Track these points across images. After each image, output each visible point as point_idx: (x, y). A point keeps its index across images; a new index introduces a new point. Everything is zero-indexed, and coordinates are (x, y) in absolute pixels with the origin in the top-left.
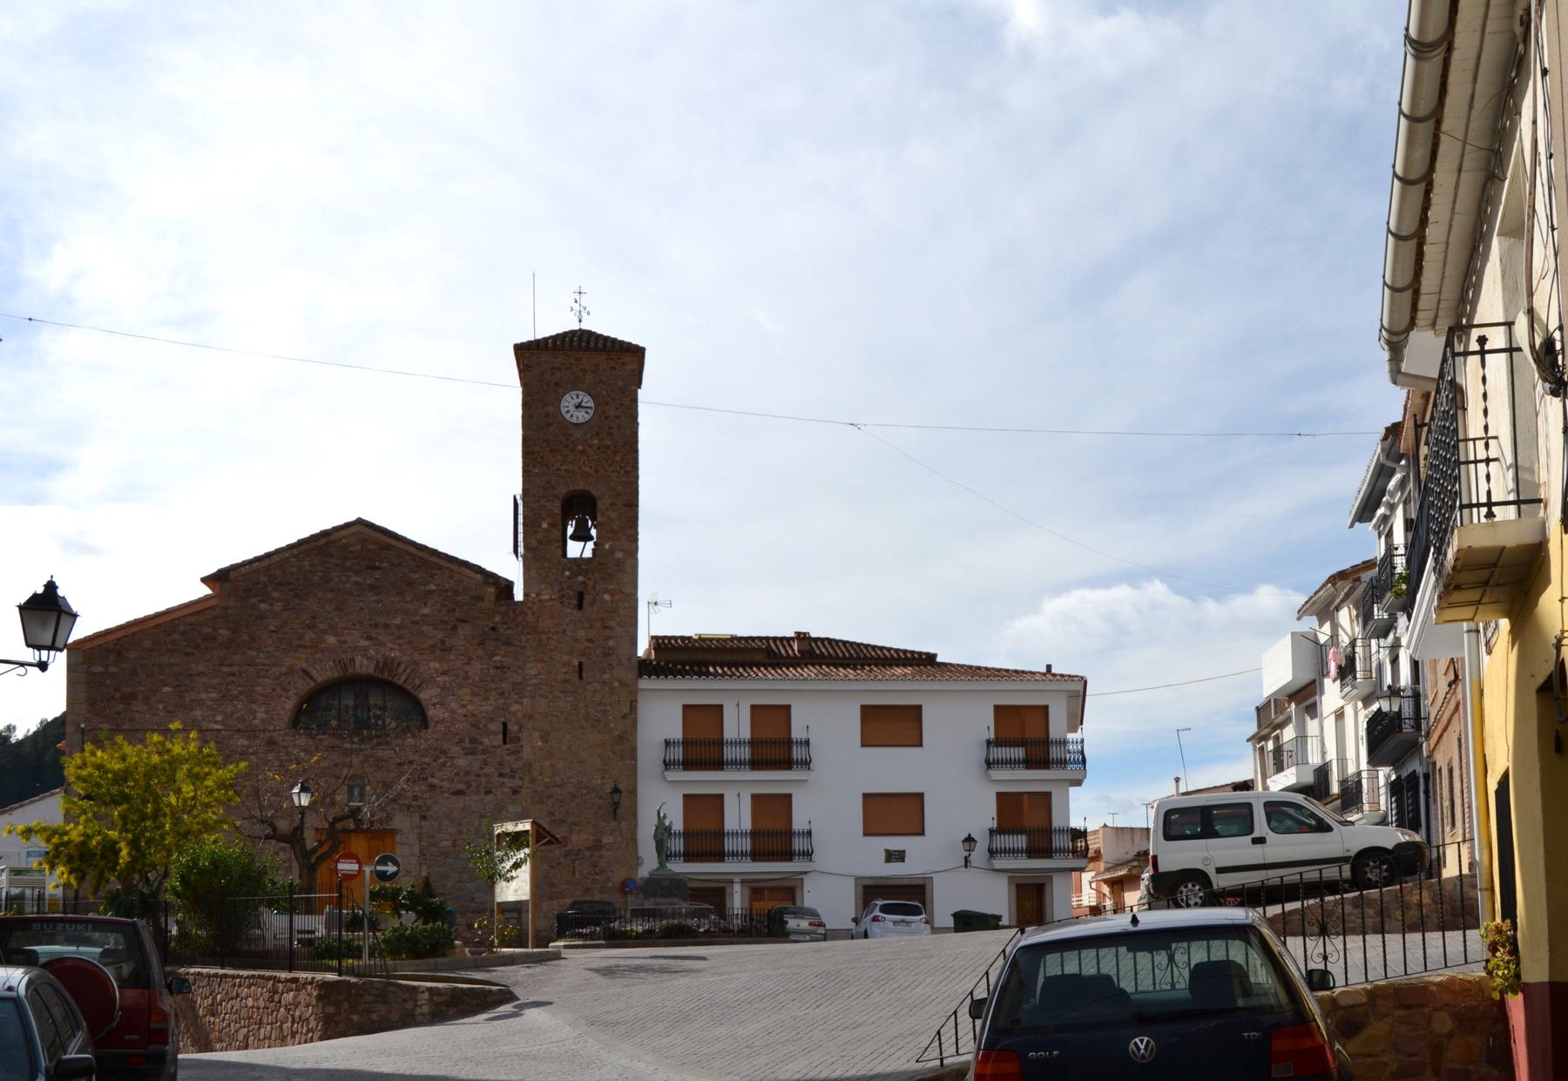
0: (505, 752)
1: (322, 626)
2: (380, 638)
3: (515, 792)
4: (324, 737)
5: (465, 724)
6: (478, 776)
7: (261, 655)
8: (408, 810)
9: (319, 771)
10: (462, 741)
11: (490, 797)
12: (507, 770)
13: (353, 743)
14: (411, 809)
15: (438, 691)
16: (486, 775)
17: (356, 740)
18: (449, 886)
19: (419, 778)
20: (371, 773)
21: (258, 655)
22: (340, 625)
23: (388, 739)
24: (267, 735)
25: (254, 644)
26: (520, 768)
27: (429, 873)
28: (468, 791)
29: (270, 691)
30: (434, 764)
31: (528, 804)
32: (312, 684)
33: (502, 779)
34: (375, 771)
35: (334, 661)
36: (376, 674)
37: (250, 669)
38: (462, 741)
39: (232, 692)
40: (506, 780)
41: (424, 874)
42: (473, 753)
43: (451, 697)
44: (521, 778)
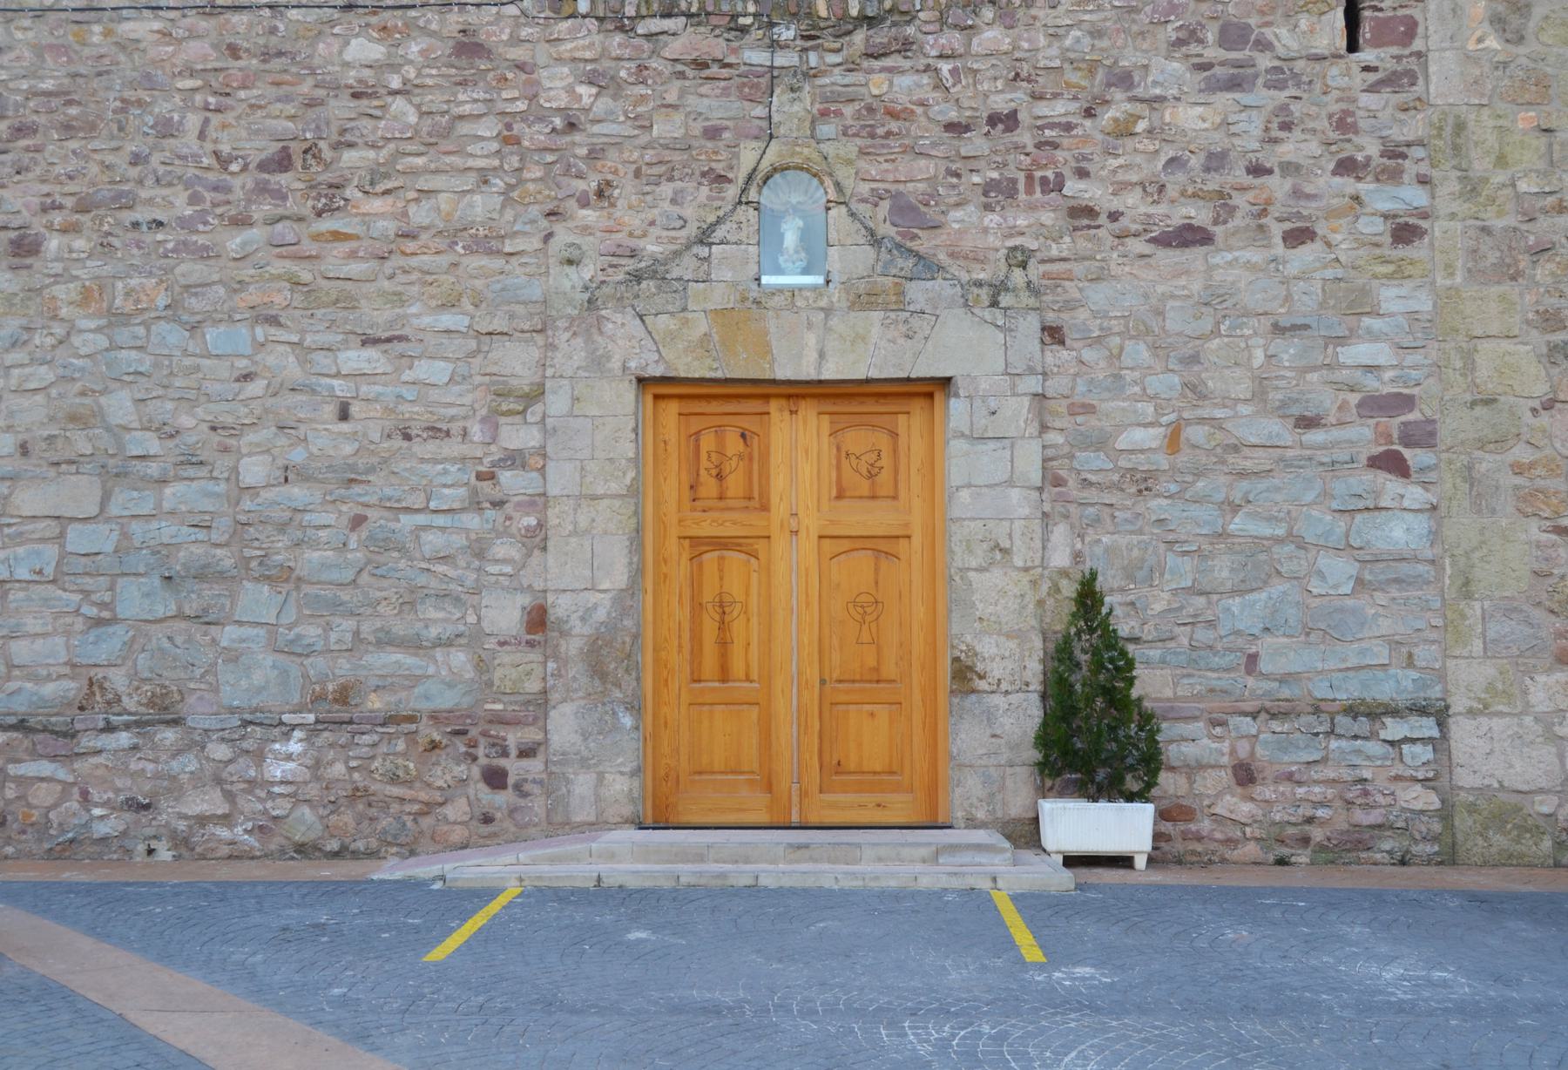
0: (1359, 80)
3: (1405, 233)
4: (668, 24)
6: (1257, 170)
9: (649, 156)
10: (1191, 36)
11: (1307, 254)
12: (1369, 148)
14: (1005, 300)
16: (1289, 168)
17: (786, 33)
18: (1158, 607)
19: (1030, 178)
20: (849, 162)
23: (910, 30)
26: (1420, 143)
28: (1218, 231)
30: (1088, 123)
31: (1458, 279)
33: (1348, 184)
34: (863, 153)
38: (1191, 36)
40: (1365, 187)
41: (1060, 558)
42: (1234, 84)
44: (1423, 181)
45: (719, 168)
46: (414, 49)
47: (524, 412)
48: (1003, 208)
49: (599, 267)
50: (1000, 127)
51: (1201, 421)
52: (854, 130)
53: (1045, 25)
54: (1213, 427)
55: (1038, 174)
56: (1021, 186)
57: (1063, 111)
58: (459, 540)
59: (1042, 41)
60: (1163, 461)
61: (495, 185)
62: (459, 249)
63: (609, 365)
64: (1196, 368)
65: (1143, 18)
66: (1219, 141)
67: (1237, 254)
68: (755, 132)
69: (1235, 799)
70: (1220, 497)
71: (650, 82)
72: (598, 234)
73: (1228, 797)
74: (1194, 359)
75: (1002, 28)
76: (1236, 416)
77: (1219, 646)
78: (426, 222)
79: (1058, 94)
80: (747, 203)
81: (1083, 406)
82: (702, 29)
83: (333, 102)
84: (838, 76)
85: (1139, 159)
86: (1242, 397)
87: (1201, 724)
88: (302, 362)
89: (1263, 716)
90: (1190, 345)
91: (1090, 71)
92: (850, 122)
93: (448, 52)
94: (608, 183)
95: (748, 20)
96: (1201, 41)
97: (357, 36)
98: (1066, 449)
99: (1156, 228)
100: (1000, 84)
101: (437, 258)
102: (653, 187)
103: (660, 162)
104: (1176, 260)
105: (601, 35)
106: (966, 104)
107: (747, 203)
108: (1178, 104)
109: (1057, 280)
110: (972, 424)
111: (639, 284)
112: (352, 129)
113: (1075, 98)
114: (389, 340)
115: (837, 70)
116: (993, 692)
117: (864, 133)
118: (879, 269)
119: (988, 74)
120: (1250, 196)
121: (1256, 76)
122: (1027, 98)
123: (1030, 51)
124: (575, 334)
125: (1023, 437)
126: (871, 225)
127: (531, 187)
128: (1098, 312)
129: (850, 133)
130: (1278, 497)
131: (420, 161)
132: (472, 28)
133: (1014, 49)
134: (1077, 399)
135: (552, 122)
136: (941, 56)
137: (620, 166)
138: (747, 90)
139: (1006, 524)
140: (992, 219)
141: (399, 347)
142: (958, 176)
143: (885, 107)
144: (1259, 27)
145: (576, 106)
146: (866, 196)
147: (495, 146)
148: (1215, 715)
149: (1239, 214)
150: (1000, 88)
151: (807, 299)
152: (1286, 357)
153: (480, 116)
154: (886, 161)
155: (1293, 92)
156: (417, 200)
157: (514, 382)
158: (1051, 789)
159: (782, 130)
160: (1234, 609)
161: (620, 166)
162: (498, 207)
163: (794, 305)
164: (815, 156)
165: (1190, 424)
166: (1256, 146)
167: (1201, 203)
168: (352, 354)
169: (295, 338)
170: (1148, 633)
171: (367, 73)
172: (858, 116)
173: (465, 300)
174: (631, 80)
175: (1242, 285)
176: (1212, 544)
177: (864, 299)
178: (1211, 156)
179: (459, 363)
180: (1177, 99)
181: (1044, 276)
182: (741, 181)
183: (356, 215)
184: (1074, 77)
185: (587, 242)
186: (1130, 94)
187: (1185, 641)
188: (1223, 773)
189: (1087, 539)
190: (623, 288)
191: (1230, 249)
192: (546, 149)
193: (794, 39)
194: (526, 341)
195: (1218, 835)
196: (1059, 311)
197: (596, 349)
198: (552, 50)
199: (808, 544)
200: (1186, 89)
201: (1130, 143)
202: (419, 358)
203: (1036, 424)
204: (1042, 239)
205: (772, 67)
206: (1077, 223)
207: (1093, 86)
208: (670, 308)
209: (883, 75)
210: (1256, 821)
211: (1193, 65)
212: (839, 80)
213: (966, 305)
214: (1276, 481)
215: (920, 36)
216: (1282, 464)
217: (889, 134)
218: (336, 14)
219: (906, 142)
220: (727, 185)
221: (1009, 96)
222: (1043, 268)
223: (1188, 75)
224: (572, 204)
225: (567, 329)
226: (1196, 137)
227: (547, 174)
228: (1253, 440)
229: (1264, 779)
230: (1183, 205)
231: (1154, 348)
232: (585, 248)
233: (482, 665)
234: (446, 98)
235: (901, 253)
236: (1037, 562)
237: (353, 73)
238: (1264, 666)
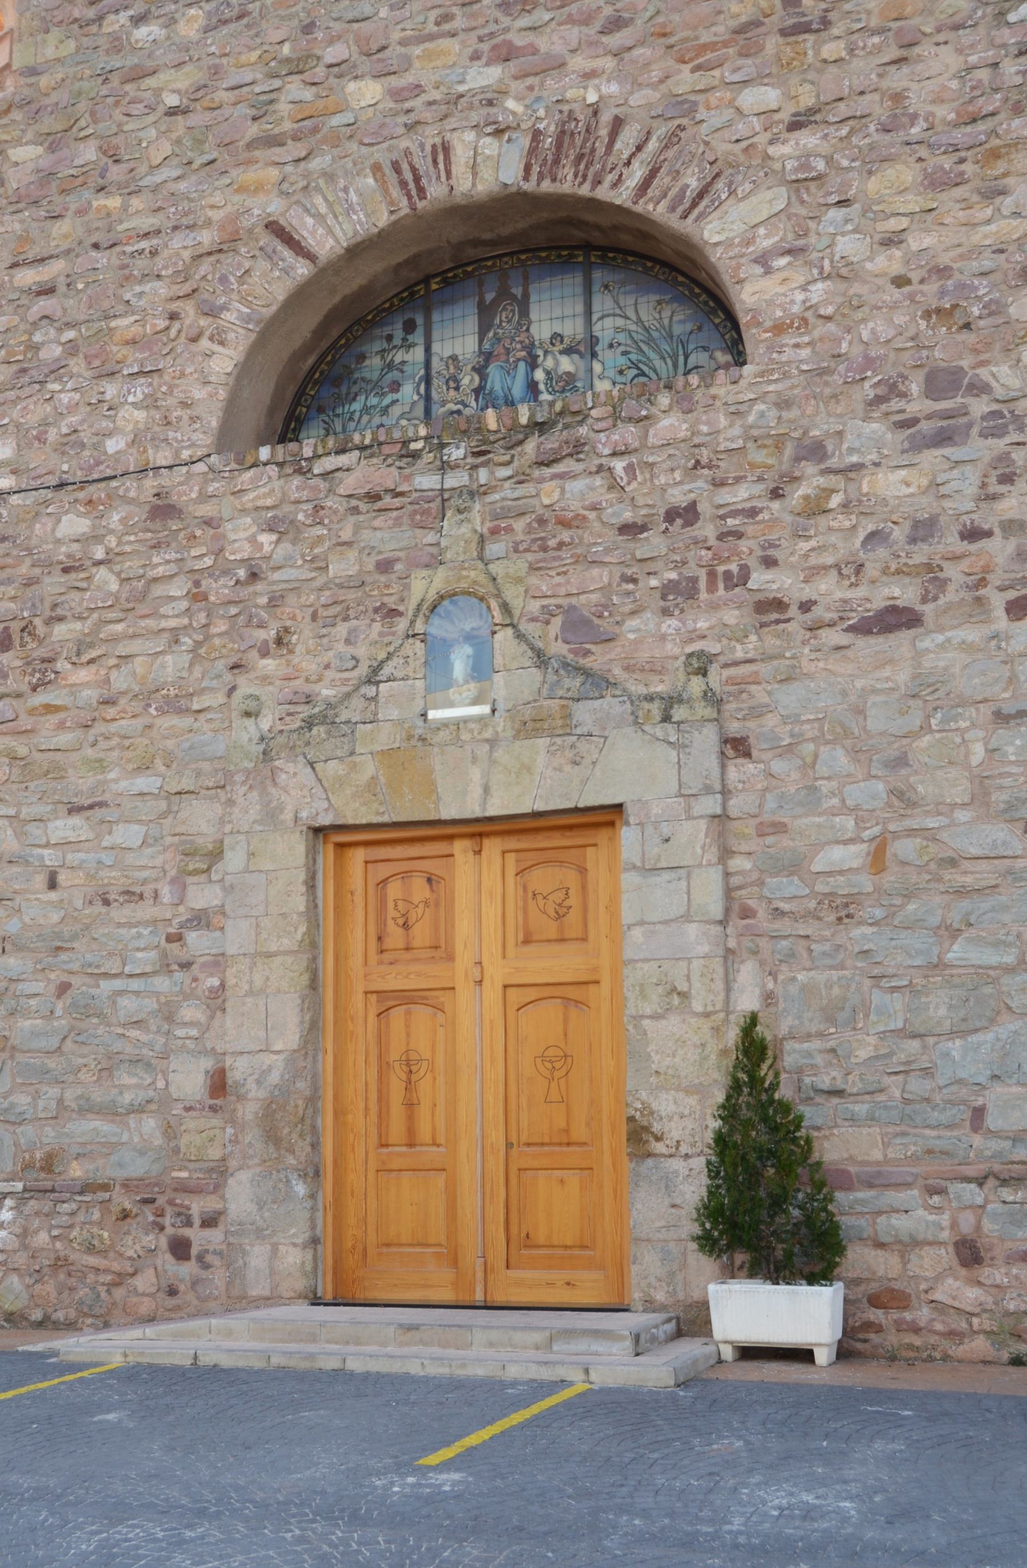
1: (333, 53)
2: (543, 43)
4: (343, 460)
5: (900, 319)
6: (973, 534)
7: (136, 203)
8: (666, 718)
9: (325, 597)
10: (893, 390)
13: (445, 467)
14: (679, 713)
15: (776, 198)
18: (863, 1054)
19: (712, 575)
20: (519, 580)
21: (125, 208)
22: (396, 35)
23: (583, 431)
24: (150, 483)
25: (116, 173)
27: (769, 998)
28: (928, 609)
29: (162, 324)
30: (776, 505)
32: (303, 270)
34: (533, 568)
35: (377, 169)
36: (529, 187)
37: (102, 259)
38: (893, 390)
39: (43, 354)
41: (747, 1001)
42: (943, 439)
43: (835, 214)
45: (391, 602)
46: (115, 518)
47: (208, 870)
48: (682, 611)
49: (277, 717)
50: (679, 522)
51: (911, 832)
52: (525, 546)
53: (726, 404)
54: (926, 839)
55: (721, 569)
56: (702, 584)
57: (746, 495)
58: (151, 1004)
59: (723, 421)
60: (866, 883)
61: (185, 643)
62: (152, 711)
63: (282, 817)
64: (903, 772)
65: (837, 379)
66: (926, 506)
67: (949, 634)
68: (426, 559)
69: (958, 1283)
70: (935, 920)
71: (326, 521)
72: (278, 683)
73: (950, 1281)
74: (901, 761)
75: (680, 414)
76: (953, 824)
77: (938, 1098)
78: (124, 687)
79: (741, 478)
80: (413, 636)
81: (775, 825)
82: (375, 460)
83: (47, 580)
84: (508, 491)
85: (833, 539)
86: (959, 801)
87: (915, 1192)
88: (19, 834)
89: (991, 1182)
90: (896, 746)
91: (777, 447)
92: (520, 537)
93: (144, 517)
94: (286, 630)
95: (419, 445)
96: (903, 395)
97: (67, 512)
98: (755, 876)
99: (854, 614)
100: (678, 475)
101: (134, 721)
102: (329, 629)
103: (335, 603)
104: (877, 648)
105: (282, 481)
106: (640, 501)
107: (413, 636)
108: (878, 469)
109: (741, 685)
110: (644, 855)
111: (310, 730)
112: (62, 603)
113: (760, 479)
114: (91, 807)
115: (507, 484)
116: (671, 1156)
117: (535, 548)
118: (545, 692)
119: (664, 466)
120: (964, 565)
121: (970, 425)
122: (706, 486)
123: (706, 435)
124: (251, 787)
125: (700, 865)
126: (540, 644)
127: (217, 641)
128: (788, 717)
129: (521, 548)
130: (1007, 918)
131: (119, 627)
132: (165, 490)
133: (693, 434)
134: (767, 817)
135: (235, 574)
136: (614, 454)
137: (298, 611)
138: (418, 517)
139: (683, 964)
140: (671, 625)
141: (98, 813)
142: (634, 581)
143: (556, 516)
144: (973, 368)
145: (258, 555)
146: (537, 614)
147: (184, 604)
148: (931, 1182)
149: (951, 588)
150: (678, 479)
151: (471, 731)
152: (1011, 749)
153: (172, 576)
154: (558, 574)
155: (1015, 437)
156: (117, 666)
157: (200, 840)
158: (741, 1267)
159: (449, 555)
160: (954, 1053)
161: (298, 611)
162: (187, 665)
163: (459, 739)
164: (482, 578)
165: (899, 837)
166: (970, 505)
167: (907, 580)
168: (59, 823)
169: (12, 812)
170: (853, 1084)
171: (75, 546)
172: (529, 530)
173: (158, 761)
174: (308, 522)
175: (957, 670)
176: (926, 977)
177: (530, 725)
178: (917, 524)
179: (151, 825)
180: (877, 464)
181: (730, 681)
182: (410, 613)
183: (66, 686)
184: (758, 456)
185: (267, 693)
186: (823, 466)
187: (897, 1094)
188: (943, 1251)
189: (781, 977)
190: (295, 736)
191: (941, 629)
192: (230, 602)
193: (465, 458)
194: (211, 798)
195: (939, 1327)
196: (744, 719)
197: (270, 802)
198: (237, 502)
199: (492, 993)
200: (886, 452)
201: (822, 521)
202: (117, 822)
203: (714, 849)
204: (725, 641)
205: (442, 490)
206: (765, 618)
207: (781, 463)
208: (339, 753)
209: (554, 483)
210: (985, 1311)
211: (894, 423)
212: (509, 494)
213: (636, 723)
214: (1004, 898)
215: (592, 435)
216: (1010, 878)
217: (561, 545)
218: (49, 494)
219: (579, 551)
220: (397, 619)
221: (687, 487)
222: (726, 673)
223: (889, 436)
224: (254, 654)
225: (244, 783)
226: (899, 505)
227: (232, 627)
228: (974, 851)
229: (992, 1259)
230: (886, 584)
231: (855, 753)
232: (264, 698)
233: (170, 1131)
234: (142, 562)
235: (568, 672)
236: (719, 1007)
237: (63, 549)
238: (992, 1121)
